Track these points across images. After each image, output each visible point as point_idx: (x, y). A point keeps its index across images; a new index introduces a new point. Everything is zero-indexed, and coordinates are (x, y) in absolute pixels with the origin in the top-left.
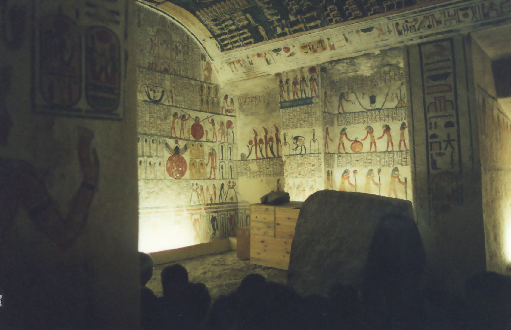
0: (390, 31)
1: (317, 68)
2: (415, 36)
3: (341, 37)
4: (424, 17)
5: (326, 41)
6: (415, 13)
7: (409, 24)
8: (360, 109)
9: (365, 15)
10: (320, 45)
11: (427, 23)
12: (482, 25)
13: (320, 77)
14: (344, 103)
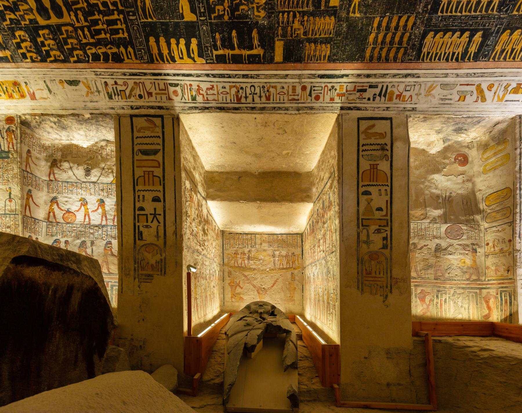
0: (99, 92)
1: (16, 119)
2: (125, 104)
3: (42, 85)
4: (135, 83)
5: (23, 85)
6: (125, 75)
7: (119, 88)
8: (74, 179)
9: (65, 61)
10: (17, 89)
11: (138, 93)
12: (191, 108)
13: (18, 129)
14: (56, 171)
